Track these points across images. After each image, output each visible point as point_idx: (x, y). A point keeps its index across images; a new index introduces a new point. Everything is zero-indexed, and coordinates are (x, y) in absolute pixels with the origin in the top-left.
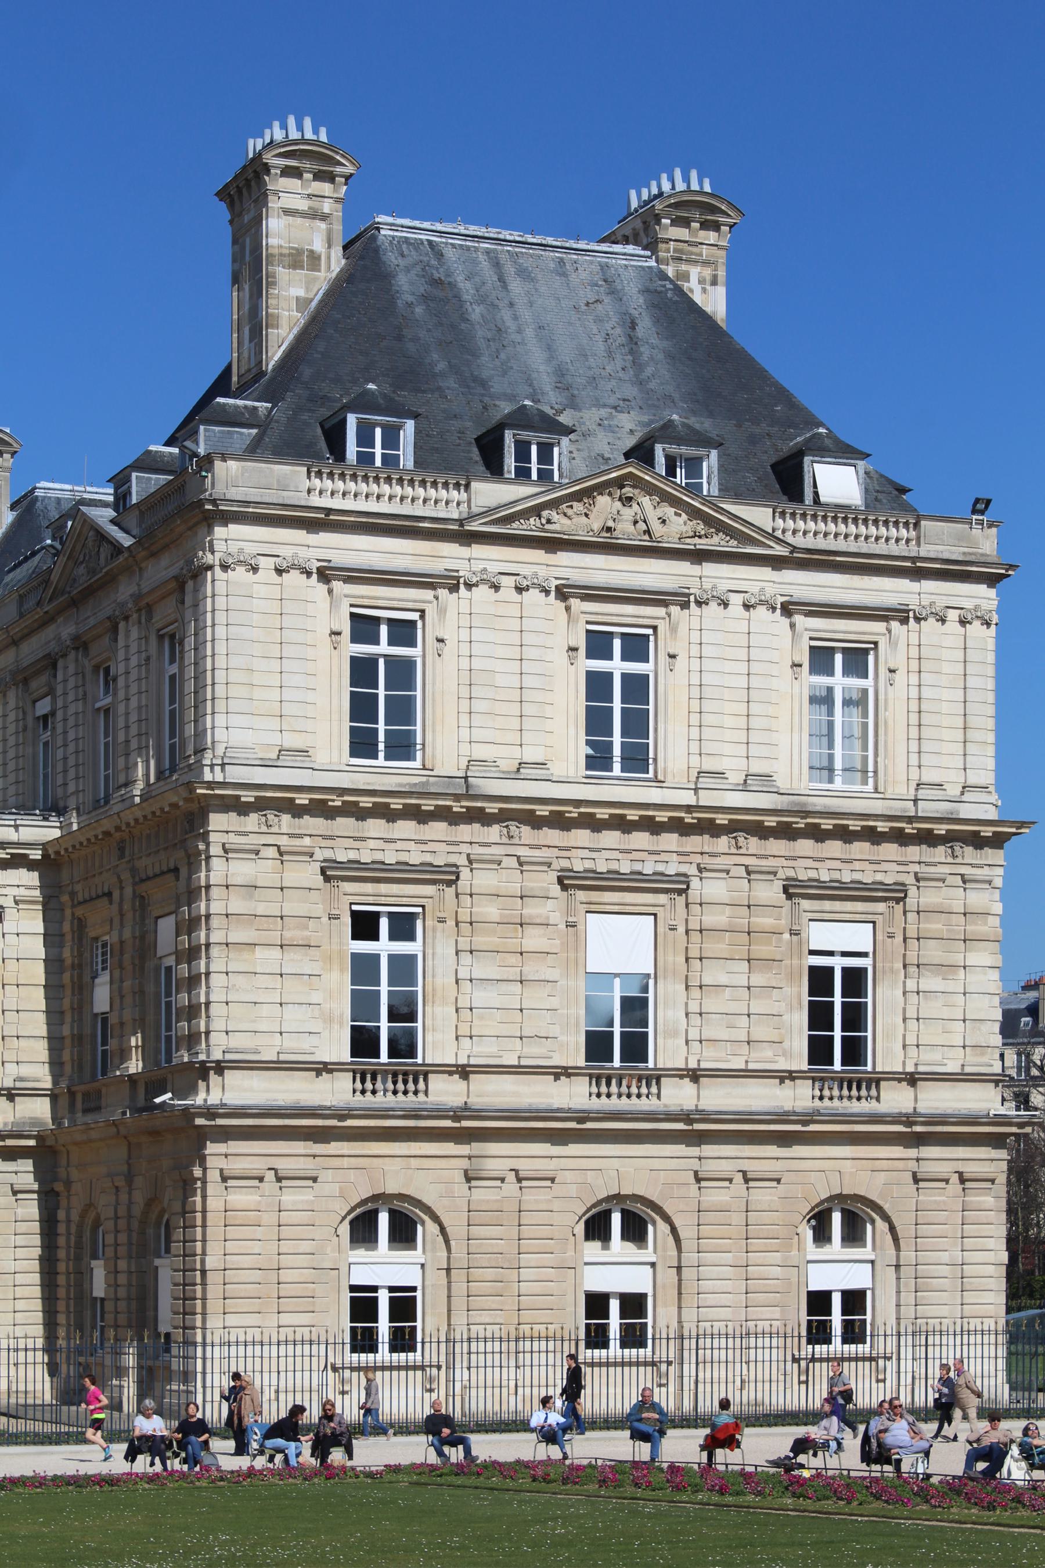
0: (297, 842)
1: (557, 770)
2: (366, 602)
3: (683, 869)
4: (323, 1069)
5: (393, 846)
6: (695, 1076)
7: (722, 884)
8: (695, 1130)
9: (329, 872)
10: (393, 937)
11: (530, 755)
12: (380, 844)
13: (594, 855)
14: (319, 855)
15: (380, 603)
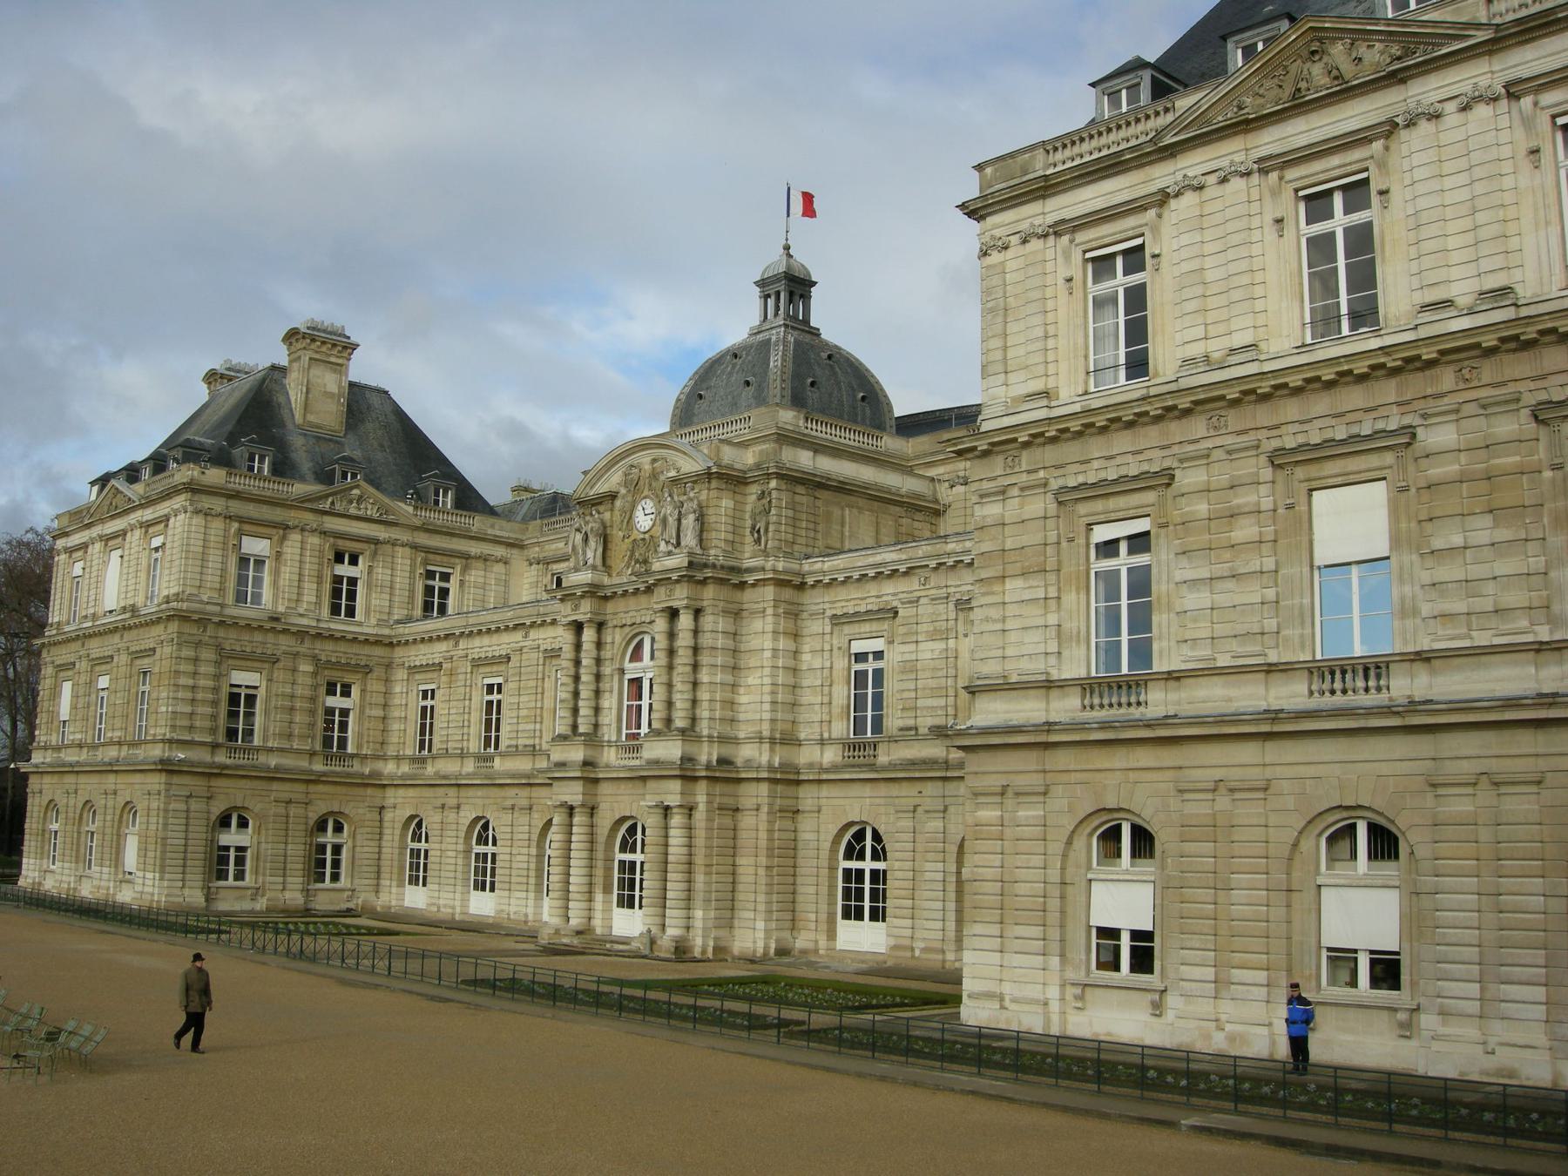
0: (1033, 476)
1: (1274, 346)
2: (1094, 244)
3: (1407, 420)
4: (1049, 685)
5: (1113, 462)
6: (1423, 657)
7: (1452, 427)
8: (1418, 722)
9: (1067, 498)
10: (1131, 552)
11: (1239, 340)
12: (1102, 463)
13: (1305, 427)
14: (1055, 484)
15: (1107, 240)
